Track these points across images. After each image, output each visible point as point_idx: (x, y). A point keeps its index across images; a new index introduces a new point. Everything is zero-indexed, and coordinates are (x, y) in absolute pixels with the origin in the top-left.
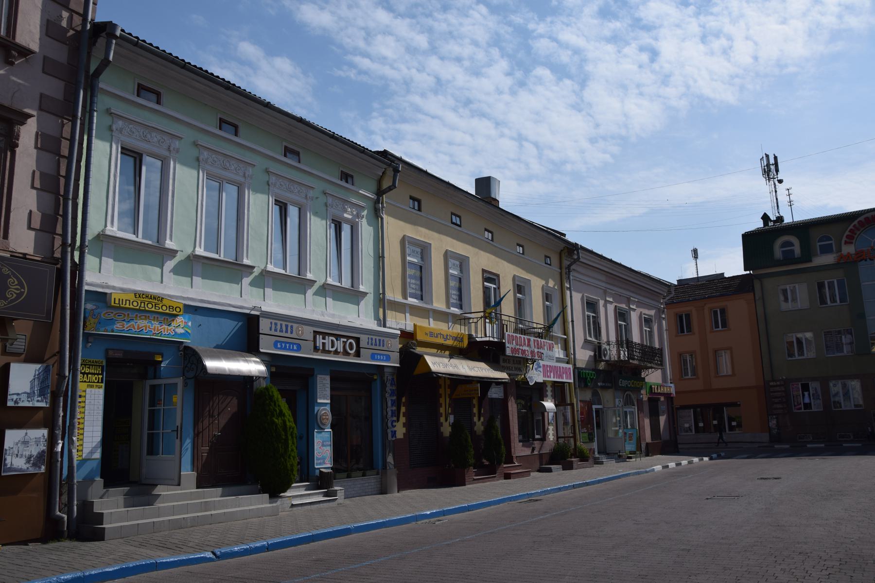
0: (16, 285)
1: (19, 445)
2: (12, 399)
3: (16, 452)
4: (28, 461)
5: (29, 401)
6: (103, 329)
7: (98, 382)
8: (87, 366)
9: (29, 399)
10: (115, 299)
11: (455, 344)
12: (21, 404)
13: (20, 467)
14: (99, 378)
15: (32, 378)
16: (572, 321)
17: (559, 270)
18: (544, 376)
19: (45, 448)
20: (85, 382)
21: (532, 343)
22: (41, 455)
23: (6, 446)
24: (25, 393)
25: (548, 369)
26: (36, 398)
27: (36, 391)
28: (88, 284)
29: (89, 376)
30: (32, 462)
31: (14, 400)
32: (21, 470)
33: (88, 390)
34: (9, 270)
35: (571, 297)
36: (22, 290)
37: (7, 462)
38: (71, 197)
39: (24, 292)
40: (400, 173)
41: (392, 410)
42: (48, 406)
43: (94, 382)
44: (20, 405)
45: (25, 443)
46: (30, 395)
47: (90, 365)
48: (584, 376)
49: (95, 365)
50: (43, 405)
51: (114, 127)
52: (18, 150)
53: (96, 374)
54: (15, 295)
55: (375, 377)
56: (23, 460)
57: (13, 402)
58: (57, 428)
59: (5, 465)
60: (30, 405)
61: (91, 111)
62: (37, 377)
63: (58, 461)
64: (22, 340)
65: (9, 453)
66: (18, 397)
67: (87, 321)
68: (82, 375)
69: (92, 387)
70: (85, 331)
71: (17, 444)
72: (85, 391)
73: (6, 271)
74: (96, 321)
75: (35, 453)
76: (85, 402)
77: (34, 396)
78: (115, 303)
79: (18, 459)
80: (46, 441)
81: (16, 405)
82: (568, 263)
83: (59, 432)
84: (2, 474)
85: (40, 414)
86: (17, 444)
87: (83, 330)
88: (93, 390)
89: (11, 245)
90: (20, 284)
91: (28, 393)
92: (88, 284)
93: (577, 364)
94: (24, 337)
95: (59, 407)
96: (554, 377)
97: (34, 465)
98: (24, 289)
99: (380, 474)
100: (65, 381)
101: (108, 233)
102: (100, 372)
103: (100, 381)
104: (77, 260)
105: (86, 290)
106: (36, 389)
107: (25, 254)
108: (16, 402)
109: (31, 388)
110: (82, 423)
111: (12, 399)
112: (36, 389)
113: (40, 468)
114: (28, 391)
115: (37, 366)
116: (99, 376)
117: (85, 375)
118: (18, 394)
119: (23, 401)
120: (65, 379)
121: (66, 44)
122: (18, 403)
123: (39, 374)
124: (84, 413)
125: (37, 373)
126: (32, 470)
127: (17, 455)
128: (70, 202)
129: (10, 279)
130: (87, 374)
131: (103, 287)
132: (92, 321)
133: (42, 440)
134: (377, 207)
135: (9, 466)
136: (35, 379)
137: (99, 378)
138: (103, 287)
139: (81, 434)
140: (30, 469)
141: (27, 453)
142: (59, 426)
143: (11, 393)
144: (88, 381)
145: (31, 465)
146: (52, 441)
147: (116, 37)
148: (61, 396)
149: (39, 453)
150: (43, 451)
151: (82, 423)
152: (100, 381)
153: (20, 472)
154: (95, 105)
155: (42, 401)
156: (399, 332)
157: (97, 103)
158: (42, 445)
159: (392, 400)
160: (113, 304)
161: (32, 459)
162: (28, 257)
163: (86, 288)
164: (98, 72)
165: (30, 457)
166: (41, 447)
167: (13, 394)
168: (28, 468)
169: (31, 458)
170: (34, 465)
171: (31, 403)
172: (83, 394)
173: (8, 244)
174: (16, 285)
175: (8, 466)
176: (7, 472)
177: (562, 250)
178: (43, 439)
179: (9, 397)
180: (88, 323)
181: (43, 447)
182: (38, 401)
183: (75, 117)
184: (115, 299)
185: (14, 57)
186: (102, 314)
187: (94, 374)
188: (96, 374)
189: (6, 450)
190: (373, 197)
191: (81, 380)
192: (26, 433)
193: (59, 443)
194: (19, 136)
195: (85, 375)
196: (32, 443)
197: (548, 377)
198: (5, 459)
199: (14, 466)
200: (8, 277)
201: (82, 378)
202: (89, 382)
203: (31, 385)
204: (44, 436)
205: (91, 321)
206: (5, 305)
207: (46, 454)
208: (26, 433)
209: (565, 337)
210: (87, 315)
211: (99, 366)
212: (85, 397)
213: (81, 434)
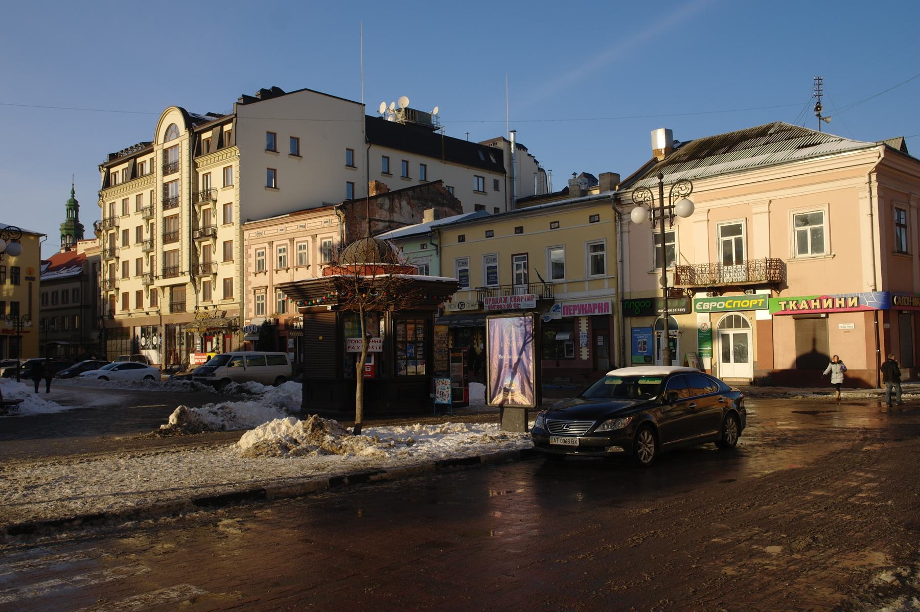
18: (564, 314)
21: (508, 300)
25: (572, 308)
48: (630, 306)
96: (579, 313)
197: (570, 314)
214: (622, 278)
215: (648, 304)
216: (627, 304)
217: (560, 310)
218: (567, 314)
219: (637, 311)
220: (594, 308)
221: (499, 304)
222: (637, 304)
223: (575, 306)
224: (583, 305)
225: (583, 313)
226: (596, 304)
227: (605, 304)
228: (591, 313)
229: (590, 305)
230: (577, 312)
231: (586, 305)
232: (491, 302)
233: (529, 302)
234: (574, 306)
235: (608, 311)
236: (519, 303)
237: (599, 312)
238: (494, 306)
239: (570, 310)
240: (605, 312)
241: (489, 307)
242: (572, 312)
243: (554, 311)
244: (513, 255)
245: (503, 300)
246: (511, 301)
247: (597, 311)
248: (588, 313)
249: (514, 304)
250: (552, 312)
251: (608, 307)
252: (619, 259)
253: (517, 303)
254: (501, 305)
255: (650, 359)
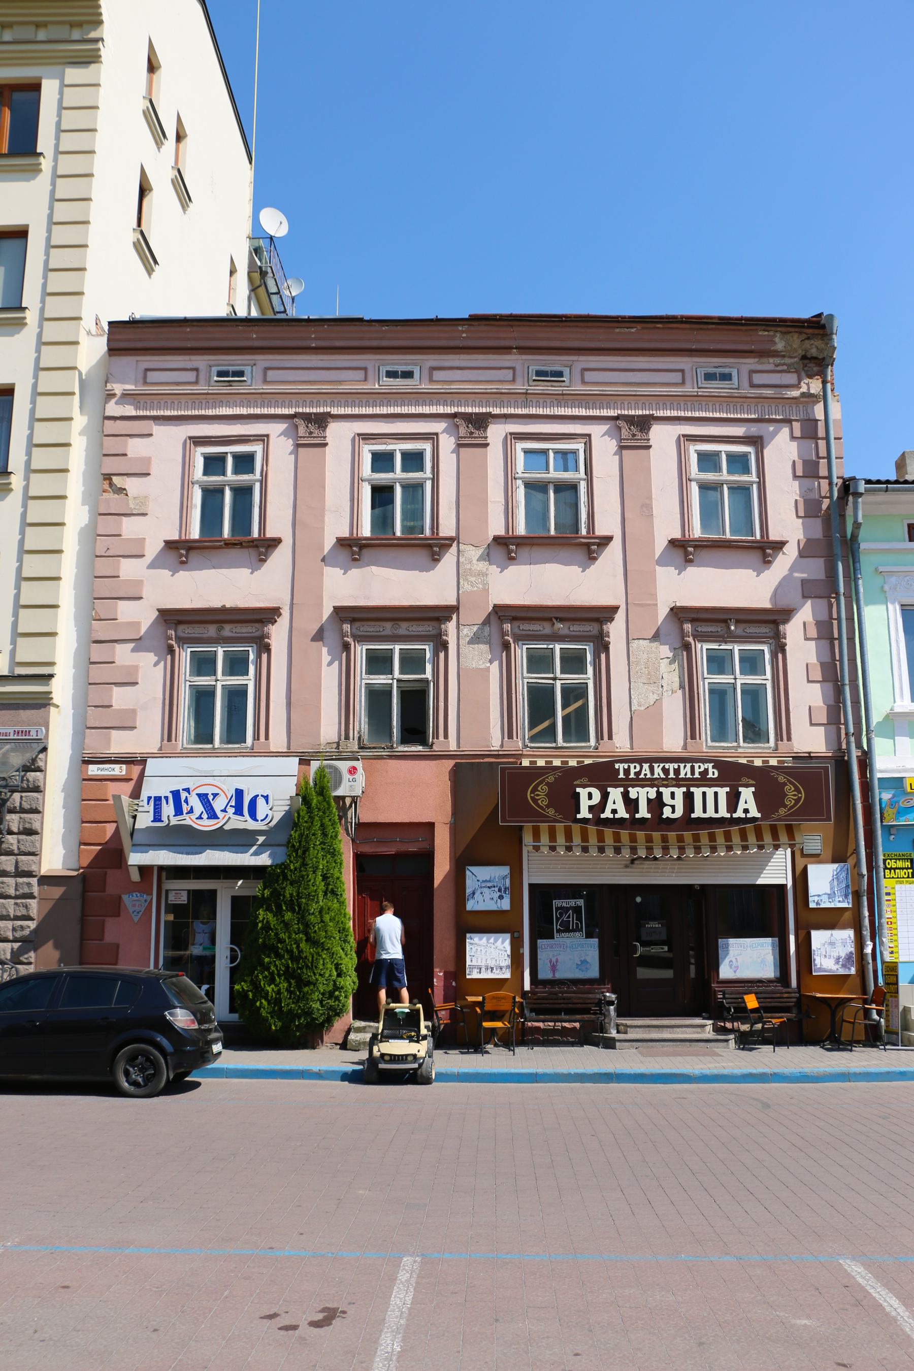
0: (793, 791)
1: (826, 946)
2: (814, 901)
3: (824, 953)
4: (837, 960)
5: (830, 902)
6: (904, 818)
7: (908, 877)
8: (893, 861)
9: (831, 900)
10: (911, 784)
12: (823, 906)
13: (830, 968)
14: (908, 873)
15: (831, 878)
19: (853, 950)
20: (893, 878)
22: (849, 957)
23: (813, 947)
24: (825, 894)
26: (837, 899)
27: (836, 892)
28: (881, 771)
29: (897, 871)
30: (841, 963)
31: (816, 901)
32: (830, 970)
33: (898, 887)
34: (785, 778)
36: (800, 795)
37: (816, 962)
38: (847, 682)
39: (801, 797)
42: (850, 906)
43: (903, 878)
44: (821, 906)
45: (832, 944)
46: (831, 896)
47: (896, 859)
49: (902, 859)
50: (845, 905)
51: (886, 588)
52: (787, 648)
53: (905, 868)
54: (793, 802)
56: (832, 961)
57: (815, 904)
58: (865, 929)
59: (815, 965)
60: (832, 905)
61: (856, 580)
62: (837, 877)
63: (869, 963)
64: (817, 841)
65: (818, 954)
66: (819, 898)
67: (885, 812)
68: (888, 871)
69: (901, 883)
70: (884, 824)
71: (824, 945)
72: (894, 888)
73: (781, 779)
74: (895, 811)
75: (843, 955)
76: (895, 900)
77: (835, 897)
78: (911, 789)
79: (827, 959)
80: (852, 942)
81: (818, 907)
83: (867, 933)
84: (814, 974)
85: (848, 915)
86: (824, 945)
87: (882, 822)
88: (903, 886)
89: (794, 745)
90: (797, 789)
91: (828, 894)
92: (881, 771)
94: (819, 838)
95: (863, 907)
97: (844, 966)
98: (801, 794)
100: (864, 881)
101: (897, 710)
102: (909, 866)
103: (910, 876)
104: (865, 748)
105: (879, 779)
106: (836, 889)
107: (809, 753)
108: (818, 903)
109: (831, 889)
110: (895, 923)
111: (814, 901)
112: (836, 889)
113: (850, 969)
114: (829, 893)
115: (835, 866)
116: (909, 870)
117: (892, 871)
118: (819, 896)
119: (824, 902)
120: (863, 877)
121: (818, 517)
122: (820, 904)
123: (837, 874)
124: (895, 911)
125: (835, 873)
126: (842, 972)
127: (825, 956)
128: (847, 689)
129: (787, 787)
130: (895, 869)
131: (899, 772)
132: (891, 811)
133: (848, 941)
135: (818, 966)
136: (833, 880)
137: (908, 873)
138: (899, 772)
139: (895, 935)
140: (840, 970)
141: (836, 955)
142: (866, 927)
143: (812, 895)
144: (896, 876)
145: (840, 966)
146: (860, 943)
147: (861, 494)
148: (863, 896)
149: (847, 955)
150: (851, 953)
151: (895, 923)
152: (910, 876)
153: (829, 972)
154: (859, 571)
155: (843, 901)
157: (860, 569)
158: (850, 946)
160: (909, 790)
161: (841, 960)
162: (812, 755)
163: (879, 775)
164: (854, 537)
165: (838, 958)
166: (848, 948)
167: (814, 896)
168: (837, 969)
169: (839, 959)
170: (844, 966)
171: (832, 903)
172: (891, 891)
173: (792, 746)
174: (793, 791)
175: (818, 967)
176: (817, 972)
178: (850, 940)
179: (810, 899)
180: (885, 815)
181: (851, 948)
182: (839, 901)
183: (837, 593)
184: (911, 784)
185: (769, 555)
186: (900, 803)
187: (903, 869)
188: (905, 868)
189: (814, 951)
191: (889, 877)
192: (832, 935)
193: (868, 945)
194: (785, 634)
195: (892, 871)
196: (839, 944)
198: (814, 960)
199: (824, 967)
200: (785, 784)
201: (889, 874)
202: (898, 878)
203: (831, 885)
204: (850, 937)
205: (889, 813)
206: (785, 812)
207: (854, 956)
208: (832, 935)
210: (883, 806)
211: (907, 859)
212: (894, 894)
213: (895, 935)
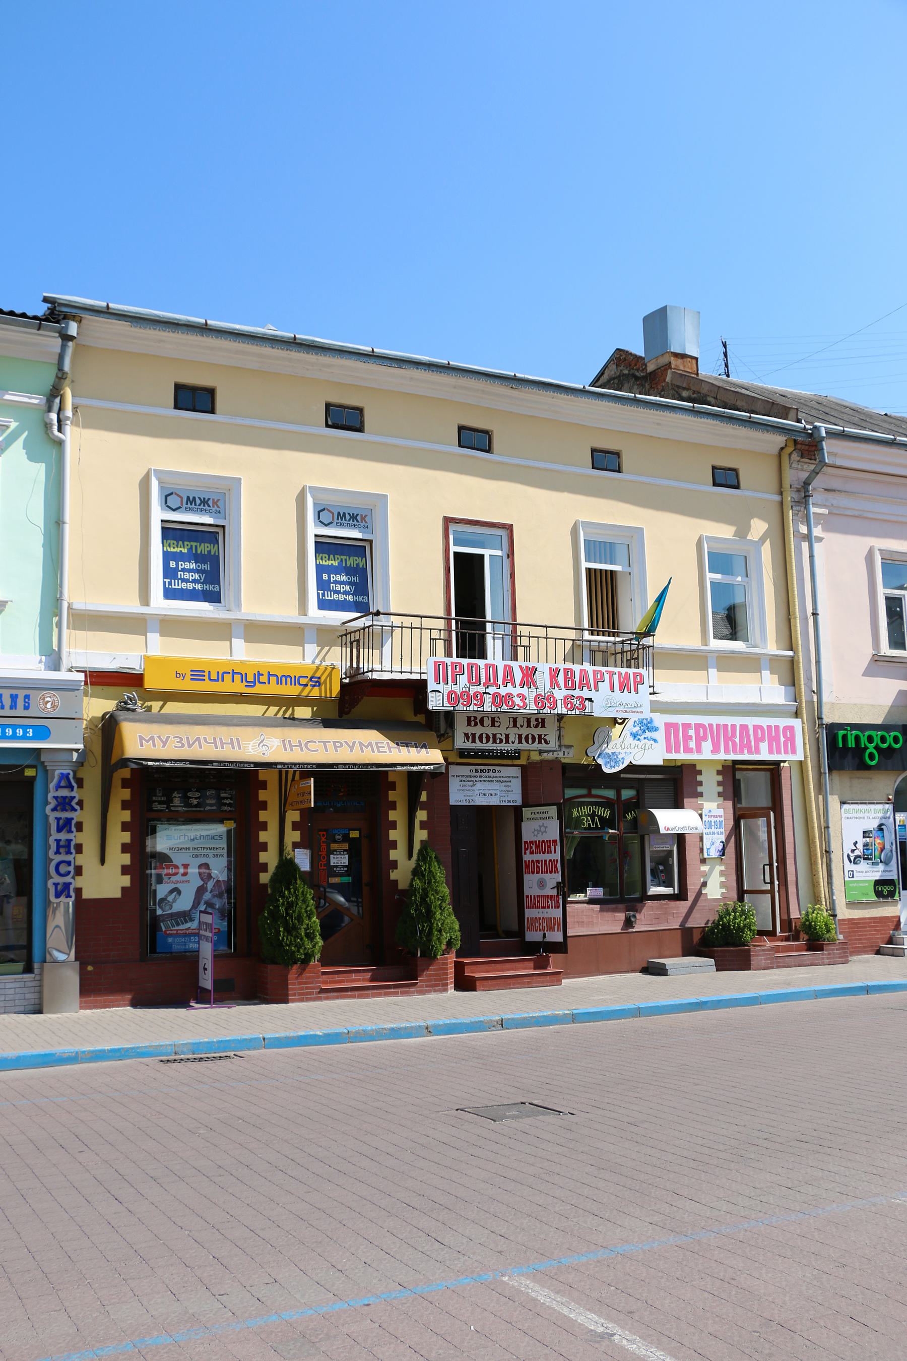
11: (305, 693)
16: (815, 614)
17: (777, 498)
18: (669, 750)
25: (691, 732)
35: (812, 557)
40: (75, 340)
41: (58, 841)
48: (851, 743)
55: (29, 773)
82: (804, 475)
93: (824, 716)
96: (716, 750)
99: (36, 971)
134: (48, 421)
156: (81, 677)
159: (58, 819)
177: (782, 449)
190: (36, 401)
197: (688, 750)
209: (791, 653)
214: (818, 662)
215: (896, 739)
216: (845, 737)
217: (654, 735)
218: (677, 751)
219: (871, 757)
220: (758, 740)
221: (503, 691)
222: (870, 739)
223: (703, 726)
224: (725, 726)
225: (727, 751)
226: (761, 727)
227: (785, 728)
228: (750, 752)
229: (744, 728)
230: (707, 746)
231: (733, 726)
232: (463, 680)
233: (627, 697)
234: (698, 726)
235: (794, 752)
236: (585, 693)
237: (771, 751)
238: (480, 698)
239: (687, 738)
240: (786, 752)
241: (452, 697)
242: (692, 744)
243: (635, 736)
244: (448, 521)
245: (518, 676)
246: (554, 683)
247: (764, 746)
248: (742, 752)
249: (565, 698)
250: (630, 740)
251: (792, 739)
252: (810, 611)
253: (577, 693)
254: (510, 696)
255: (891, 888)
